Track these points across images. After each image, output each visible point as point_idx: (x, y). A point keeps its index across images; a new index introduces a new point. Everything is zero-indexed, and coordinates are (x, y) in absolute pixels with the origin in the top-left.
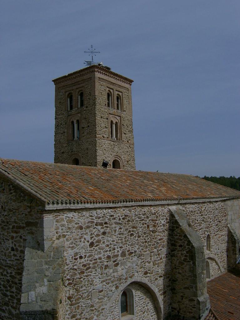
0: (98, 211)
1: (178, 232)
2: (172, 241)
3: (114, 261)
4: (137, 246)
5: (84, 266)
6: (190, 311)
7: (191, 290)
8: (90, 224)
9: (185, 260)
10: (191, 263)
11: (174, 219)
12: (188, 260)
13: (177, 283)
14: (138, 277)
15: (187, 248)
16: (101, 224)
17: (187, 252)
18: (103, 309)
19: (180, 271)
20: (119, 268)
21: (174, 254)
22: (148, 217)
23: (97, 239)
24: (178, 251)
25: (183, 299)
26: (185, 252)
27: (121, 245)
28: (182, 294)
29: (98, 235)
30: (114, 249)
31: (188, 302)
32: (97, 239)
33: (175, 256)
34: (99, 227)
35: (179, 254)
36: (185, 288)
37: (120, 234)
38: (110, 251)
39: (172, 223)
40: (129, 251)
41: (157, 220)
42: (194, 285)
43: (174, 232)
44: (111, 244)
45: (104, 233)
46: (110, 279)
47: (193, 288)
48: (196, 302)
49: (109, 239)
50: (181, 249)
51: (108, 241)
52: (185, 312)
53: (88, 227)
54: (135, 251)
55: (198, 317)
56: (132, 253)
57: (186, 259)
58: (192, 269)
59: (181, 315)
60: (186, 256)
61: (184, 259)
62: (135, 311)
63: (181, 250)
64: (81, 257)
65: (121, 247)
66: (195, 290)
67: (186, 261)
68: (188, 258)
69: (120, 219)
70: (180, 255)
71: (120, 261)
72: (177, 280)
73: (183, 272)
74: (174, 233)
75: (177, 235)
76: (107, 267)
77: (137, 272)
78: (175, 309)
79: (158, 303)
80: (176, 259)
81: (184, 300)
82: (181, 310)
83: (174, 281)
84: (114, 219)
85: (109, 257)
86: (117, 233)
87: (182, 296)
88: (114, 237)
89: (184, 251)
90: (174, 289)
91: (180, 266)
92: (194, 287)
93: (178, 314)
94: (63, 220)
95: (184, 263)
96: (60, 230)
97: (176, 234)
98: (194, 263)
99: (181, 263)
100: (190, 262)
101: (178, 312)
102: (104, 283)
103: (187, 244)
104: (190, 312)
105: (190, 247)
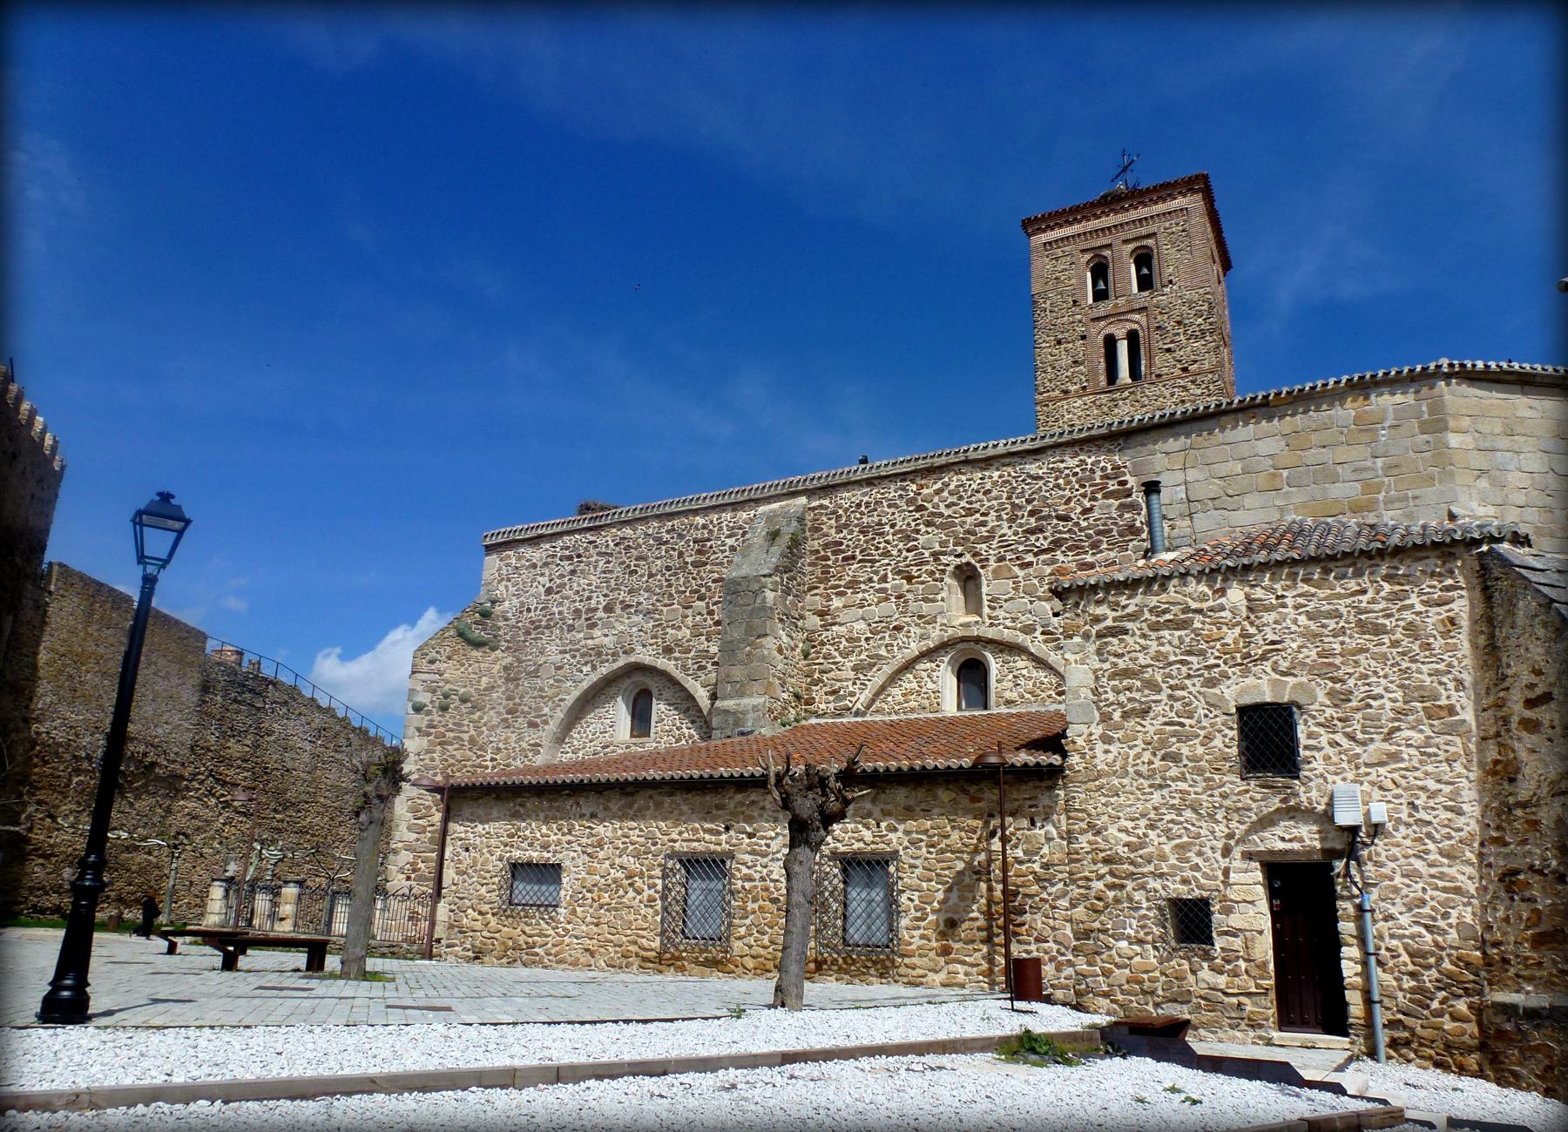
0: (566, 538)
3: (587, 619)
4: (646, 595)
5: (532, 622)
8: (550, 560)
14: (644, 656)
16: (570, 558)
18: (561, 700)
20: (597, 632)
22: (681, 536)
23: (558, 581)
27: (605, 591)
29: (562, 576)
30: (589, 598)
32: (558, 581)
34: (566, 563)
37: (604, 572)
38: (581, 601)
40: (622, 602)
41: (709, 540)
44: (584, 590)
45: (573, 572)
46: (578, 650)
49: (582, 581)
51: (579, 585)
53: (546, 564)
54: (639, 604)
56: (631, 606)
62: (653, 730)
64: (529, 610)
65: (605, 596)
69: (607, 546)
71: (600, 619)
76: (571, 628)
77: (644, 646)
84: (596, 547)
85: (577, 611)
86: (599, 569)
88: (592, 577)
94: (509, 557)
96: (504, 572)
102: (568, 656)
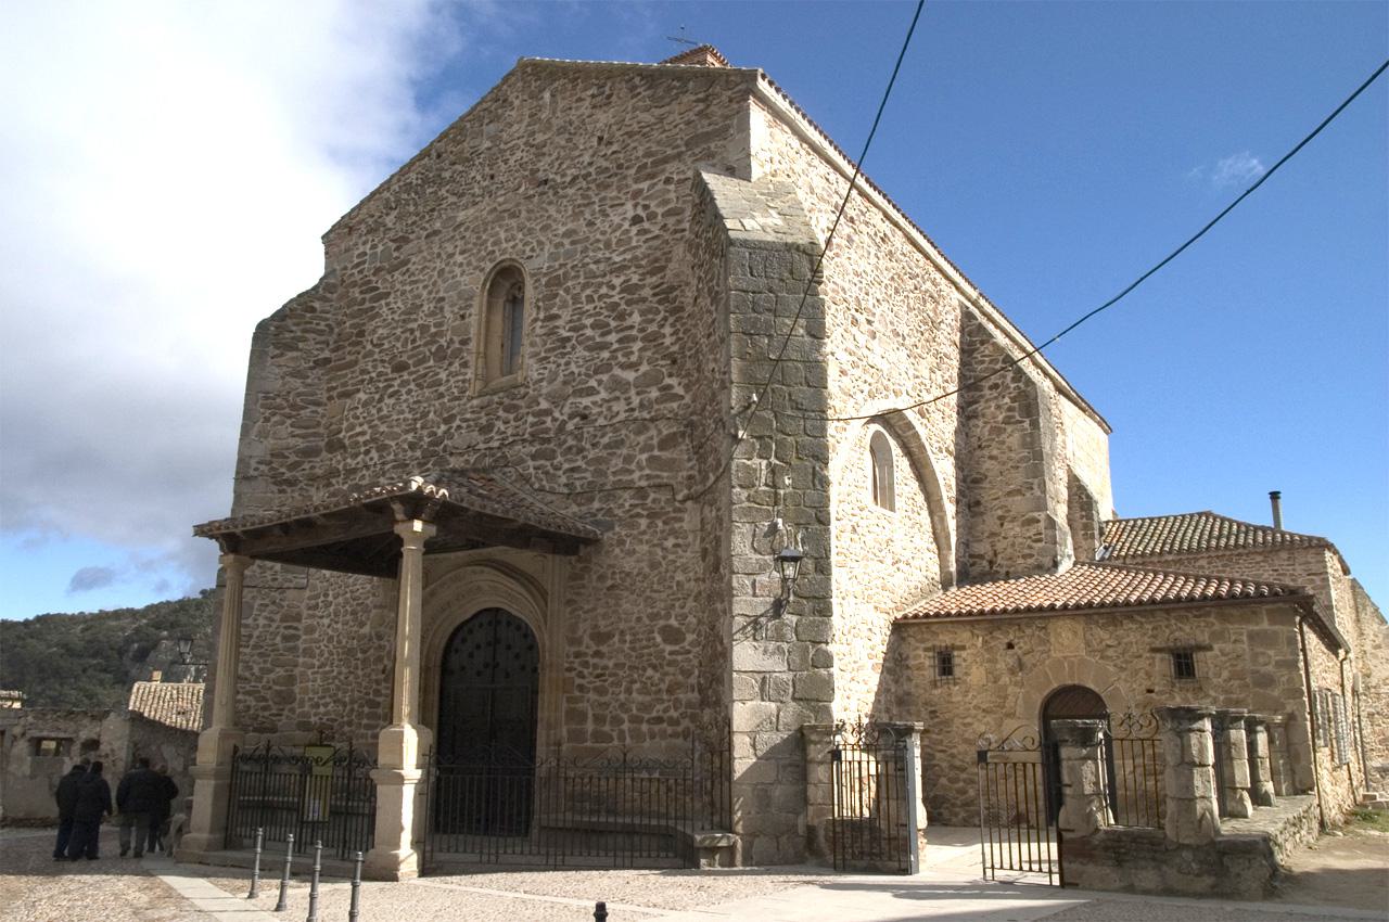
1: (987, 352)
2: (970, 378)
6: (1027, 551)
7: (1028, 495)
9: (1007, 421)
10: (1026, 424)
11: (974, 322)
12: (1018, 418)
13: (986, 484)
15: (1014, 389)
17: (1013, 400)
19: (995, 452)
21: (975, 411)
24: (987, 401)
25: (1006, 524)
26: (1007, 400)
28: (1000, 512)
31: (1018, 529)
33: (976, 417)
35: (990, 407)
36: (1009, 494)
39: (969, 335)
42: (1036, 481)
43: (975, 355)
47: (1032, 489)
48: (1042, 525)
50: (996, 395)
52: (1010, 559)
55: (1051, 564)
57: (1013, 417)
58: (1028, 439)
59: (998, 569)
60: (1010, 409)
61: (1006, 417)
63: (996, 398)
66: (1039, 493)
67: (1009, 423)
68: (1016, 414)
70: (992, 409)
72: (986, 477)
73: (1004, 453)
74: (976, 358)
75: (983, 362)
78: (981, 557)
79: (943, 519)
80: (981, 424)
81: (1007, 525)
82: (1000, 556)
83: (976, 481)
87: (1000, 518)
89: (1004, 397)
90: (978, 503)
91: (993, 440)
92: (1035, 487)
93: (991, 568)
95: (1005, 429)
97: (980, 358)
98: (1035, 424)
99: (997, 431)
100: (1024, 422)
101: (991, 563)
103: (1013, 378)
104: (1024, 557)
105: (1021, 385)
